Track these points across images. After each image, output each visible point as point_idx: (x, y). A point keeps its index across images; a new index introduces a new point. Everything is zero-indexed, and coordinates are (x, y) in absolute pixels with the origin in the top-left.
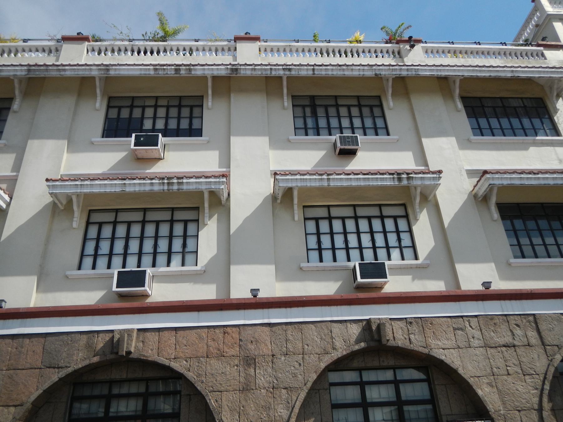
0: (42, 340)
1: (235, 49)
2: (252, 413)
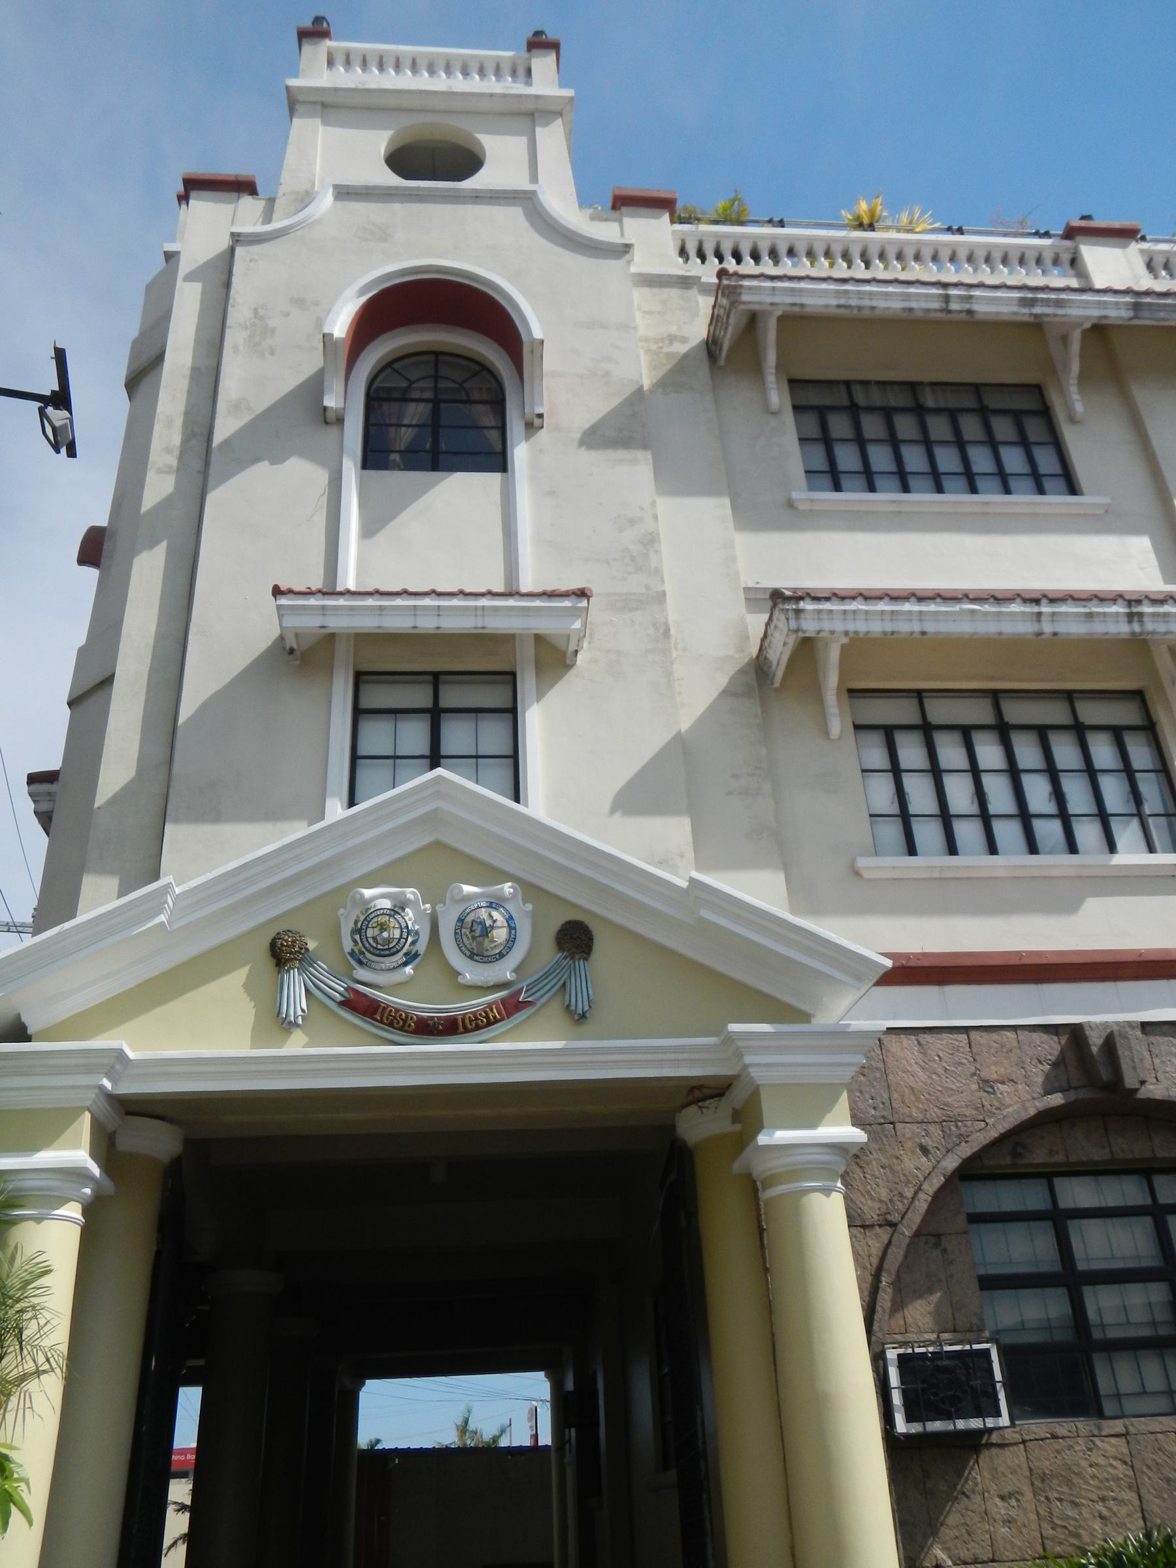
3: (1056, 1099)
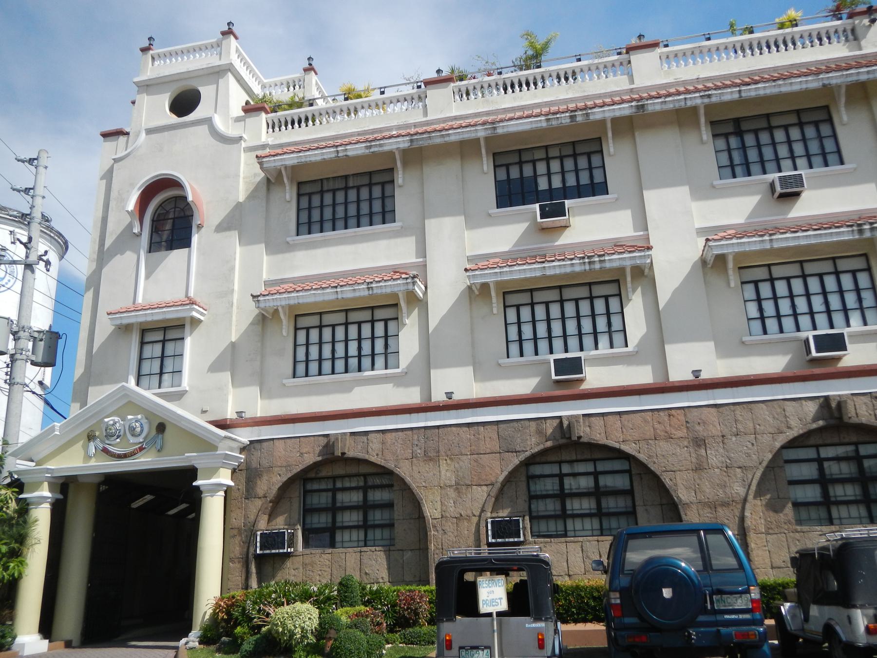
0: (495, 427)
1: (629, 62)
2: (707, 490)
3: (320, 459)
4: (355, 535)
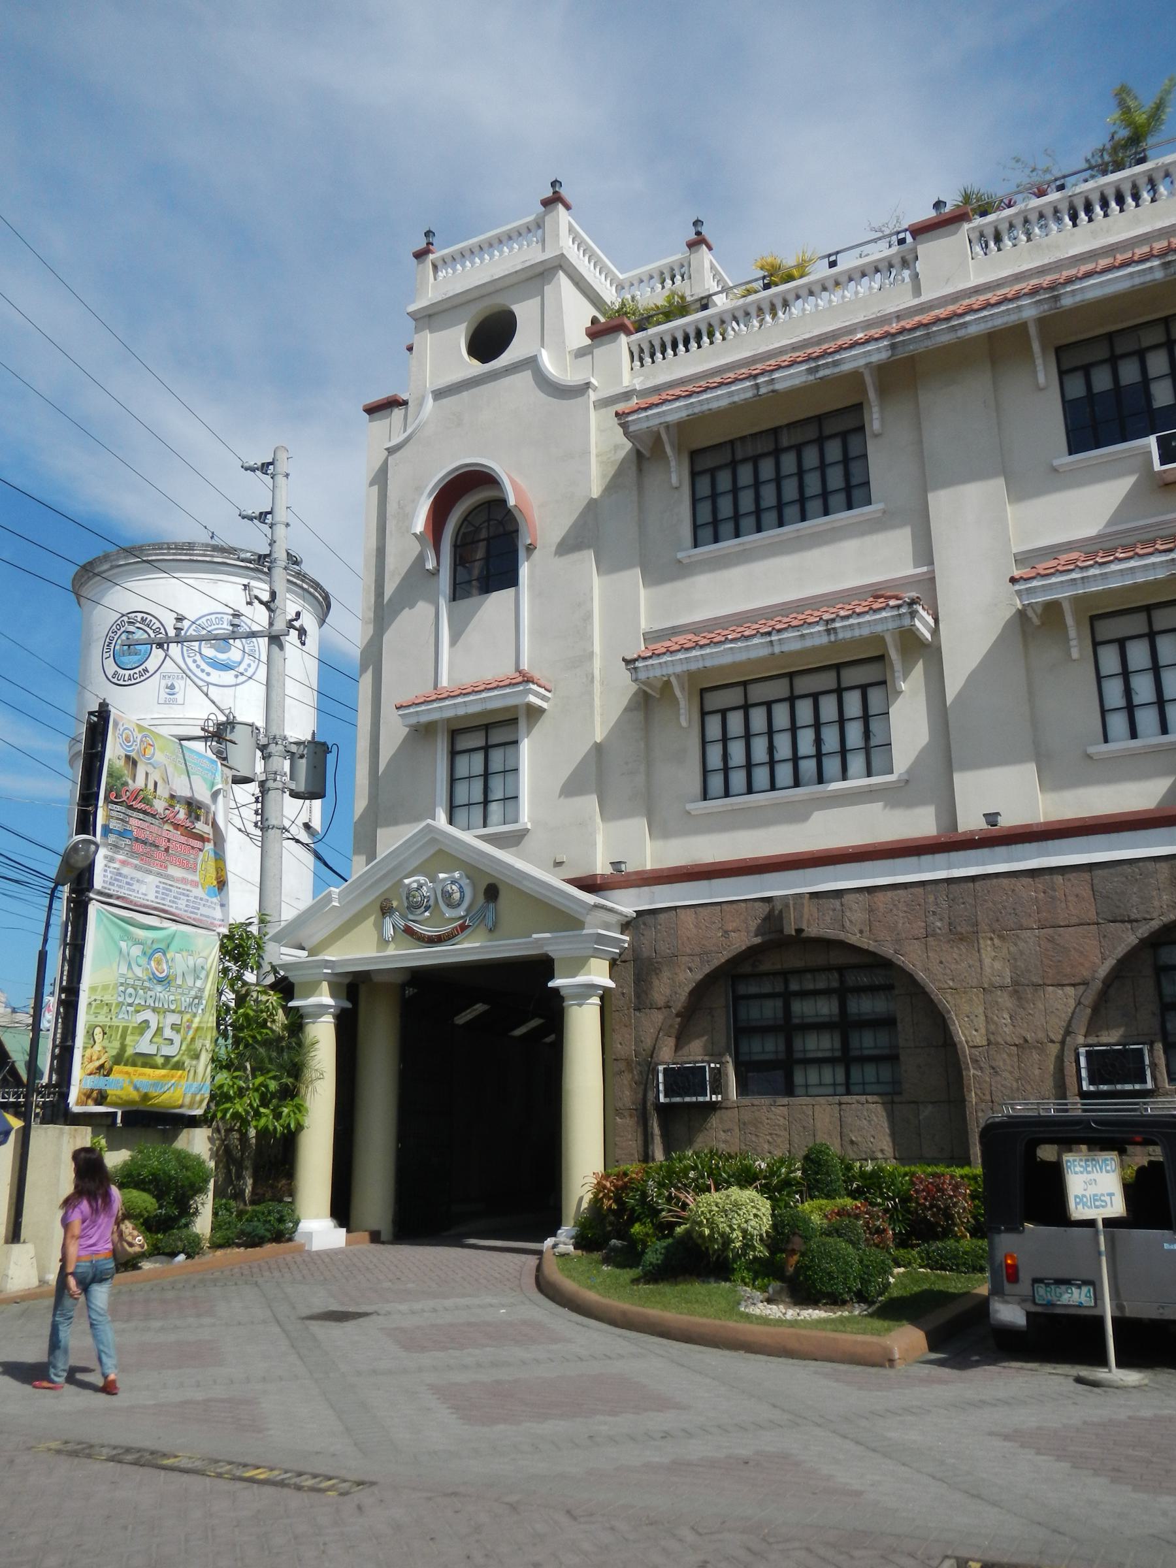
0: (1087, 876)
3: (758, 940)
4: (827, 1074)
